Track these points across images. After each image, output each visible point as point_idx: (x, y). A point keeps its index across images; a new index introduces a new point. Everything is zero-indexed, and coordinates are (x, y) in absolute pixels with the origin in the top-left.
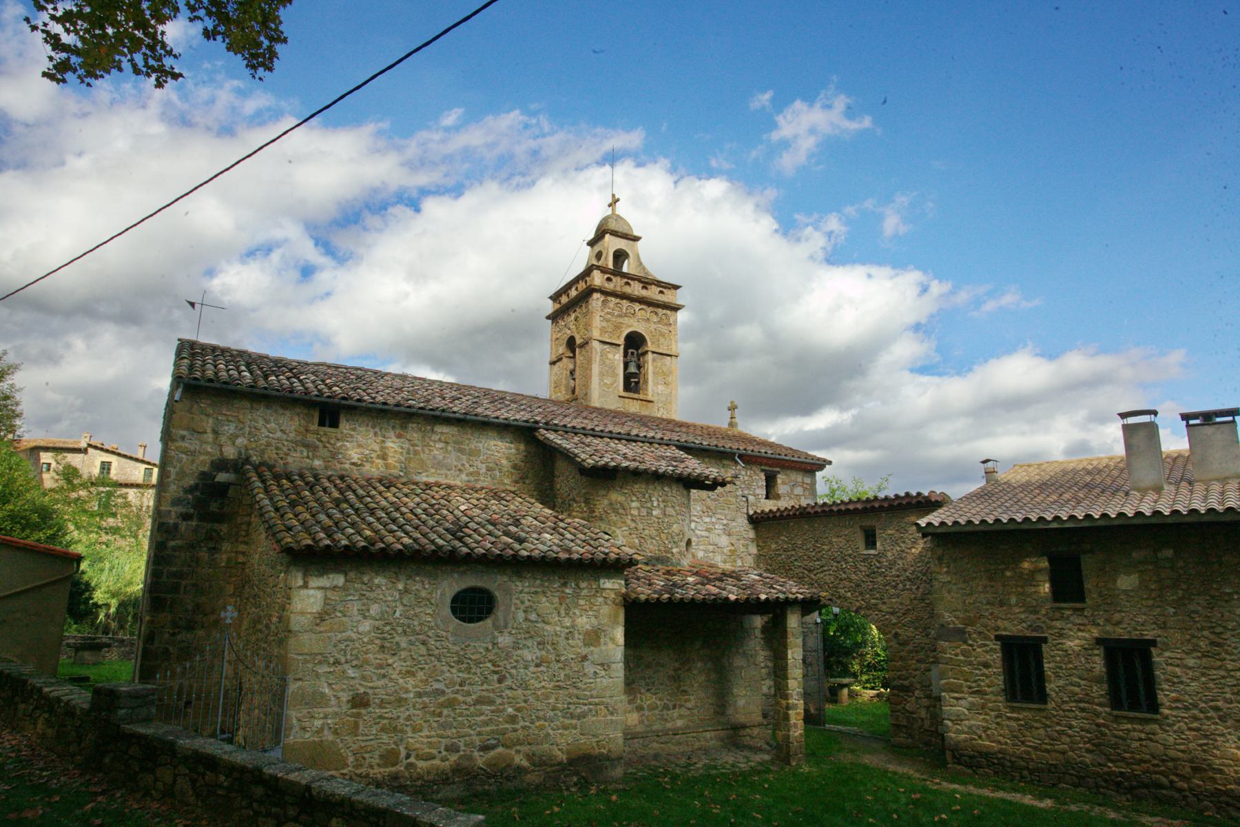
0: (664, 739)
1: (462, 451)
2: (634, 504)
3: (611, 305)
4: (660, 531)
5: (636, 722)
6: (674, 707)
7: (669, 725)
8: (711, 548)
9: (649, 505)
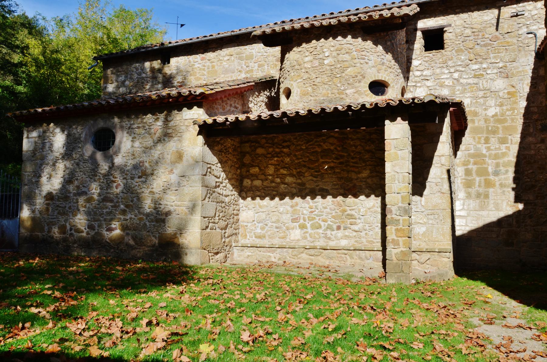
0: (312, 252)
1: (241, 59)
2: (307, 59)
4: (332, 76)
5: (298, 237)
6: (339, 228)
7: (332, 244)
8: (481, 94)
9: (321, 56)
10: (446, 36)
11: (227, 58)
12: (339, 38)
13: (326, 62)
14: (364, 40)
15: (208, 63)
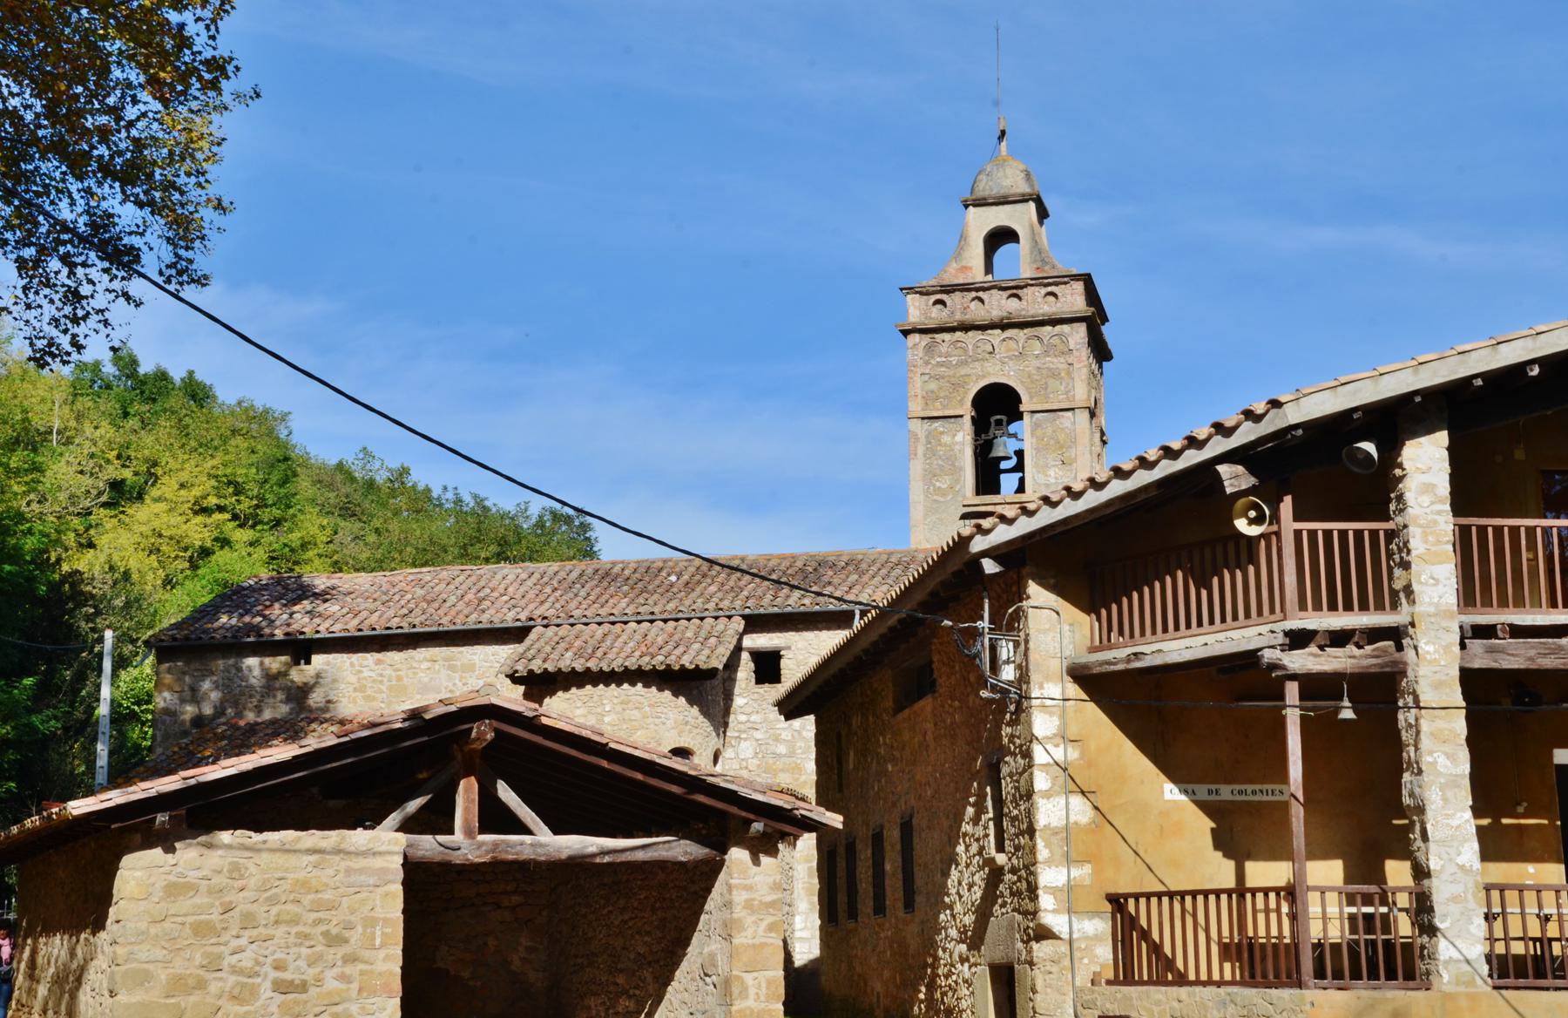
1: (452, 668)
3: (944, 348)
10: (783, 663)
11: (425, 665)
12: (626, 686)
13: (607, 719)
14: (660, 690)
15: (389, 672)
